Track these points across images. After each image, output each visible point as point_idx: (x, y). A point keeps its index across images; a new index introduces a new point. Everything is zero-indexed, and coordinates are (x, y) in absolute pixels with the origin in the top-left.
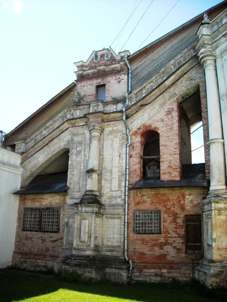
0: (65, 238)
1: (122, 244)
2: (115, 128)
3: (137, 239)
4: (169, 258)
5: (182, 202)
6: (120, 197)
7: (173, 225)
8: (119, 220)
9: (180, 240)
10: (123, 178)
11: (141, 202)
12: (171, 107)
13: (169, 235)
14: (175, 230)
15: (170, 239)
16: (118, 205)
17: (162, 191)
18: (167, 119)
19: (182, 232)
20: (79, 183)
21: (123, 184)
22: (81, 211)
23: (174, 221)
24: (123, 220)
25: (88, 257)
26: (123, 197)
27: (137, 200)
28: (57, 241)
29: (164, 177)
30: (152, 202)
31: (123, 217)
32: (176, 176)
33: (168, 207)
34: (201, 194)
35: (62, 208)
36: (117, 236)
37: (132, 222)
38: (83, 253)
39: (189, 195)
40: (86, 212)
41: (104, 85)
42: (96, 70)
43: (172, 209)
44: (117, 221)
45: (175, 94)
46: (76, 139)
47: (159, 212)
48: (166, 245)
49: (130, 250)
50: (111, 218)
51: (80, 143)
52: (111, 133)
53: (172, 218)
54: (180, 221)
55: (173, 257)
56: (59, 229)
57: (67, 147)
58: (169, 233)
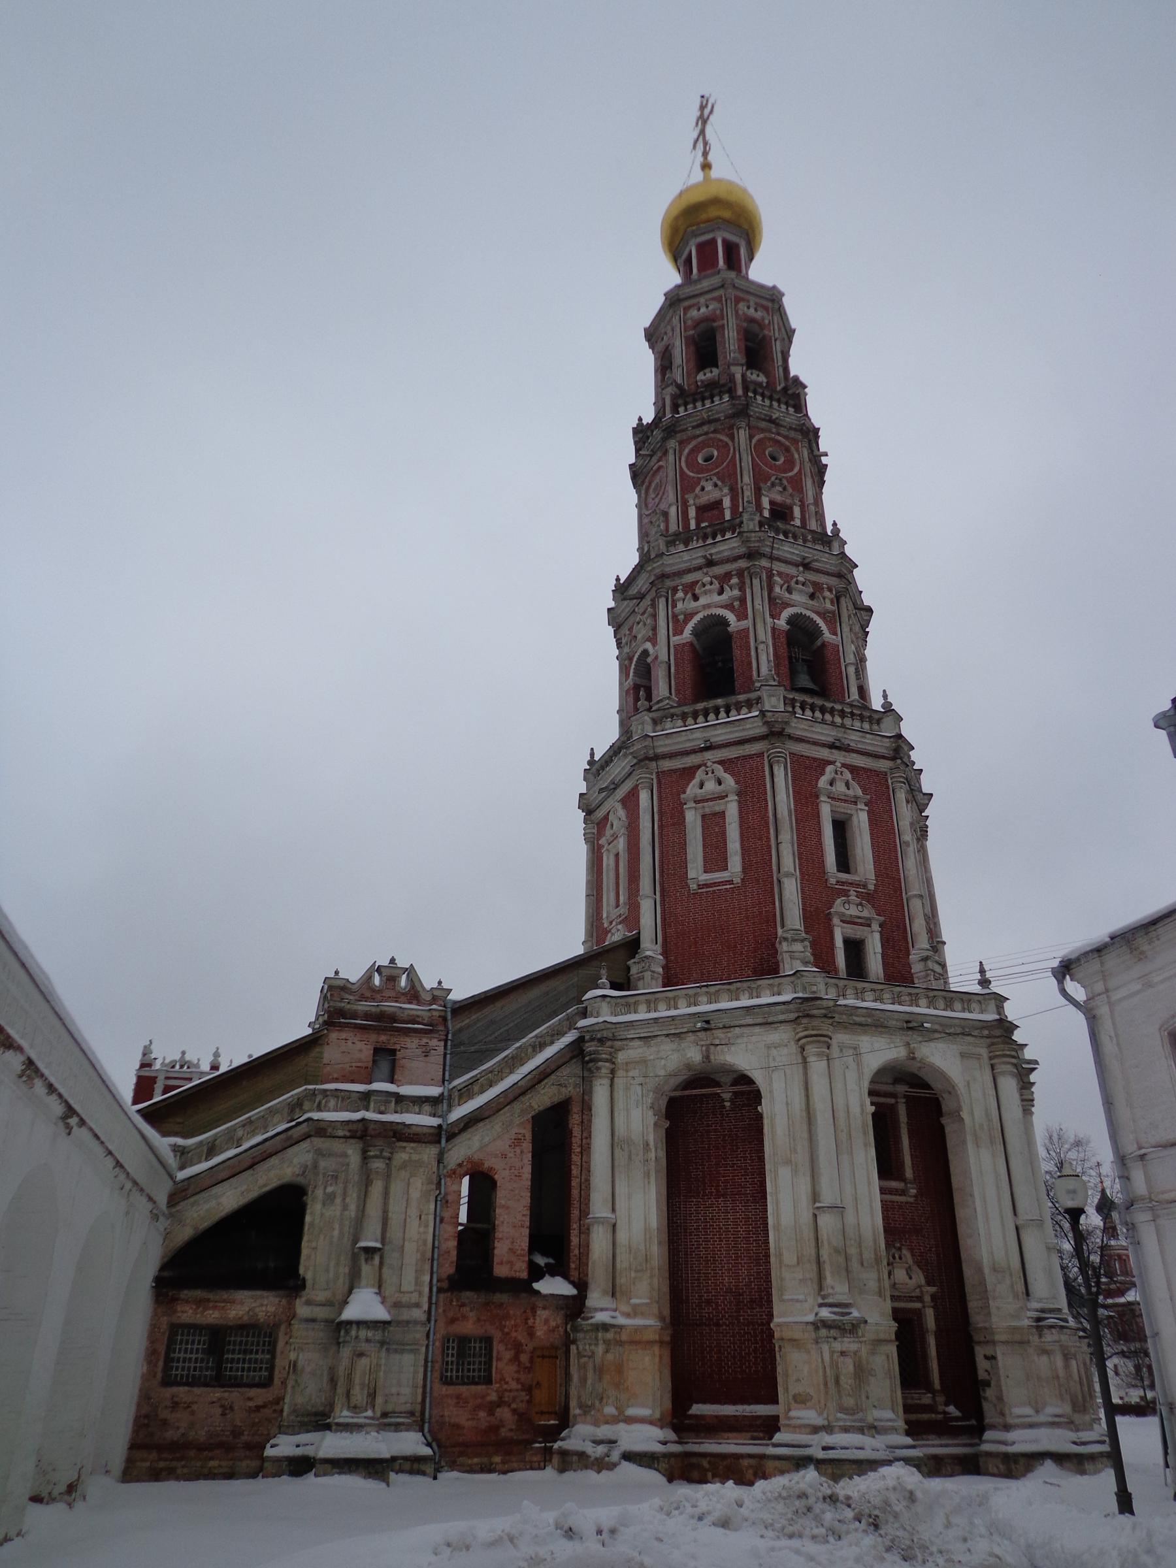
0: (287, 1400)
2: (415, 1157)
3: (447, 1396)
5: (530, 1322)
7: (514, 1368)
8: (412, 1356)
10: (427, 1267)
11: (457, 1319)
12: (522, 1131)
13: (505, 1386)
14: (516, 1376)
15: (507, 1394)
16: (416, 1322)
17: (499, 1297)
18: (512, 1155)
20: (327, 1270)
21: (427, 1278)
22: (357, 1337)
23: (516, 1358)
24: (422, 1357)
26: (426, 1307)
27: (450, 1314)
28: (264, 1406)
29: (501, 1271)
30: (479, 1320)
31: (424, 1349)
33: (506, 1330)
34: (562, 1309)
35: (283, 1327)
36: (406, 1391)
37: (439, 1358)
39: (544, 1308)
40: (368, 1341)
41: (393, 1052)
43: (514, 1334)
44: (408, 1359)
45: (531, 1107)
47: (488, 1341)
48: (499, 1406)
49: (433, 1420)
50: (396, 1351)
52: (404, 1166)
53: (513, 1352)
55: (511, 1430)
56: (271, 1378)
57: (301, 1180)
58: (507, 1383)
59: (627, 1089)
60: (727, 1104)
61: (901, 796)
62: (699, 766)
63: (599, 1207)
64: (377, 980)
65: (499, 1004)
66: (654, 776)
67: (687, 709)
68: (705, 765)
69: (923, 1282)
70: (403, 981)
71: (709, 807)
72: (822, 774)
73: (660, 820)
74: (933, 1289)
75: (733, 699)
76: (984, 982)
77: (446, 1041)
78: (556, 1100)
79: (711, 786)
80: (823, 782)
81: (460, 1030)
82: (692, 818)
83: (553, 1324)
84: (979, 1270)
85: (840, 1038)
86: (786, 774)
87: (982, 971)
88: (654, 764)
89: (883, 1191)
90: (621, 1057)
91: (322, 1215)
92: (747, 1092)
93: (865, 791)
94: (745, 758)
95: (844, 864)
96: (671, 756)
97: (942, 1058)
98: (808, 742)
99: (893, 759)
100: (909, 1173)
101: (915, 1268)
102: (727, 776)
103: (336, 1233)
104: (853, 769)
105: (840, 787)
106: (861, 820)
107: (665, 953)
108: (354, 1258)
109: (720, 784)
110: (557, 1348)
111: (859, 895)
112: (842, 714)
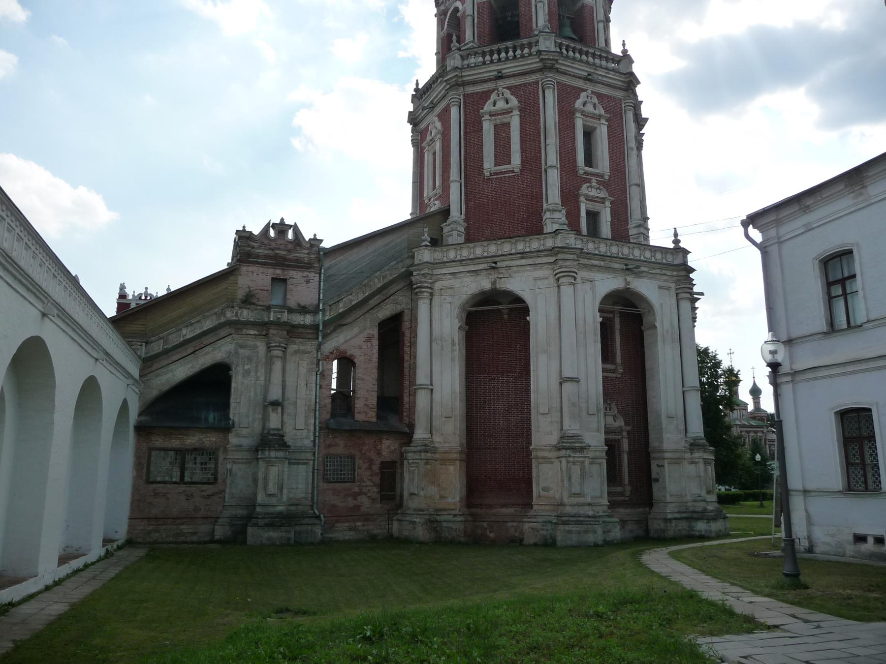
0: (227, 490)
1: (310, 495)
4: (363, 509)
5: (379, 447)
6: (307, 438)
7: (368, 473)
9: (376, 489)
10: (312, 414)
19: (377, 480)
20: (248, 416)
21: (312, 421)
23: (370, 468)
25: (280, 513)
26: (312, 439)
28: (213, 495)
32: (372, 416)
35: (221, 449)
36: (302, 486)
37: (321, 468)
38: (271, 510)
41: (284, 281)
42: (270, 252)
43: (368, 454)
44: (302, 468)
46: (241, 351)
47: (352, 457)
51: (249, 359)
53: (367, 465)
54: (376, 468)
56: (216, 479)
57: (227, 361)
59: (441, 306)
60: (506, 316)
61: (630, 115)
62: (494, 90)
63: (422, 378)
64: (272, 233)
65: (355, 251)
66: (461, 97)
67: (487, 49)
68: (497, 89)
69: (623, 423)
70: (290, 235)
71: (500, 119)
72: (578, 98)
73: (465, 128)
74: (629, 428)
75: (518, 42)
76: (676, 241)
77: (320, 274)
78: (394, 313)
79: (501, 105)
80: (578, 104)
81: (329, 268)
82: (488, 127)
83: (393, 448)
84: (659, 416)
85: (583, 274)
86: (554, 97)
87: (676, 235)
88: (461, 89)
89: (604, 370)
90: (437, 286)
91: (242, 383)
92: (519, 308)
93: (606, 111)
94: (525, 85)
95: (589, 161)
96: (474, 83)
97: (646, 287)
98: (569, 75)
99: (626, 90)
100: (619, 360)
101: (618, 415)
102: (513, 98)
103: (252, 394)
104: (599, 96)
105: (589, 108)
106: (602, 132)
107: (467, 220)
108: (265, 408)
109: (507, 103)
110: (396, 462)
111: (598, 182)
112: (594, 55)
